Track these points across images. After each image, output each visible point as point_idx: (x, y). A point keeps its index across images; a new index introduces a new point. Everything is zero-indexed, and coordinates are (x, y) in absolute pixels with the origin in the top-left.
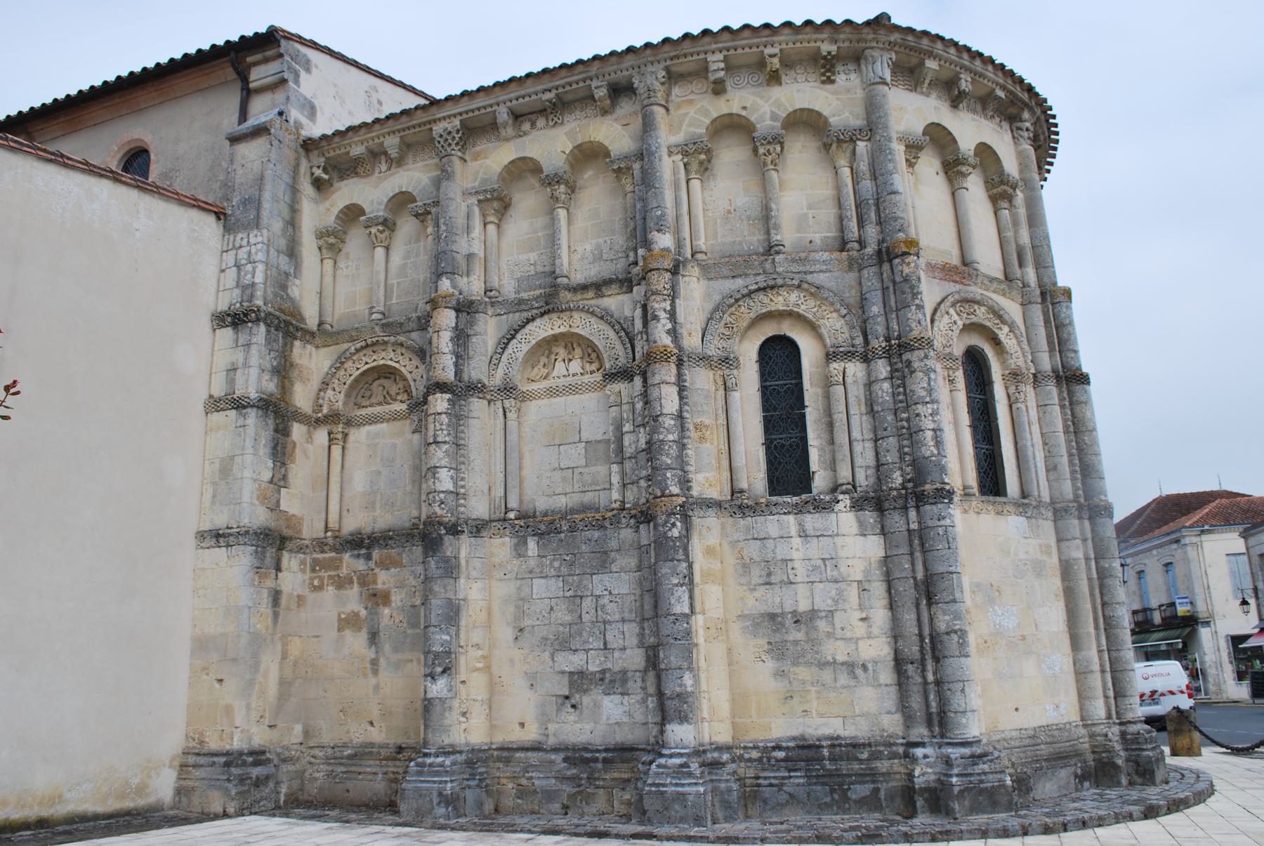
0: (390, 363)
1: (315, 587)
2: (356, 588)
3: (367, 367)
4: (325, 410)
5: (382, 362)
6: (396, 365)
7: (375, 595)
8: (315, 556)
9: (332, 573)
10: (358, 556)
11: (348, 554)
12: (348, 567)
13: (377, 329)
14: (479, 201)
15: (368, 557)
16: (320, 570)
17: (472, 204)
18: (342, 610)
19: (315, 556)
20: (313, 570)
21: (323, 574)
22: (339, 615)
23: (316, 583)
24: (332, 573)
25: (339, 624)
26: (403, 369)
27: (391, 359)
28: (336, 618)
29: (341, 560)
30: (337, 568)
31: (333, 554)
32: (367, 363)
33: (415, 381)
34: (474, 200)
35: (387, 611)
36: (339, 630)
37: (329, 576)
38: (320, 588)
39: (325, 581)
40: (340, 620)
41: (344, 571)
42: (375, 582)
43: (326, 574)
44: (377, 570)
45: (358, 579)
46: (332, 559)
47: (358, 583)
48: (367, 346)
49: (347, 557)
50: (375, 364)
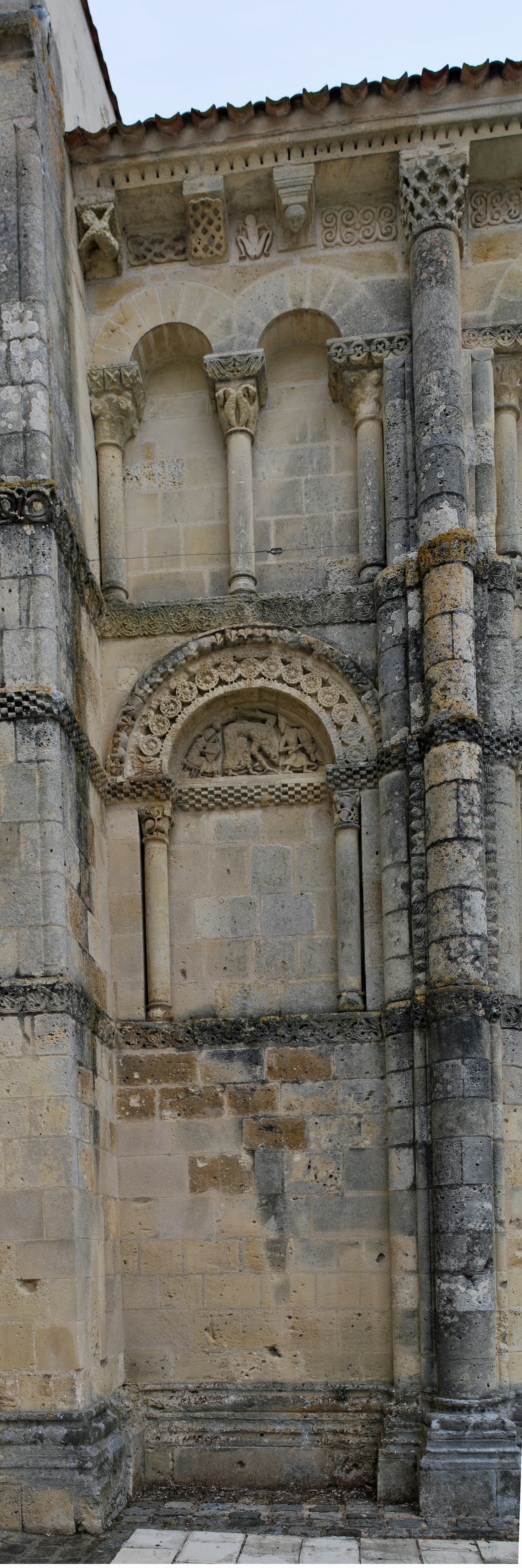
0: (277, 686)
1: (133, 1110)
2: (228, 1115)
3: (221, 690)
4: (129, 771)
5: (259, 683)
6: (294, 692)
7: (270, 1128)
8: (128, 1052)
9: (173, 1086)
10: (230, 1056)
11: (204, 1053)
12: (207, 1075)
13: (248, 610)
14: (497, 351)
15: (254, 1059)
16: (143, 1080)
17: (482, 354)
18: (198, 1153)
19: (128, 1052)
20: (127, 1079)
21: (149, 1085)
22: (193, 1162)
23: (134, 1102)
24: (173, 1086)
25: (193, 1178)
26: (308, 701)
27: (280, 679)
28: (186, 1168)
29: (190, 1062)
30: (182, 1076)
31: (170, 1051)
32: (222, 682)
33: (339, 727)
34: (486, 347)
35: (298, 1157)
36: (193, 1189)
37: (163, 1091)
38: (146, 1111)
39: (157, 1100)
40: (194, 1170)
41: (199, 1082)
42: (270, 1104)
43: (158, 1088)
44: (274, 1083)
45: (232, 1096)
46: (169, 1060)
47: (233, 1105)
48: (226, 644)
49: (202, 1056)
50: (242, 685)
